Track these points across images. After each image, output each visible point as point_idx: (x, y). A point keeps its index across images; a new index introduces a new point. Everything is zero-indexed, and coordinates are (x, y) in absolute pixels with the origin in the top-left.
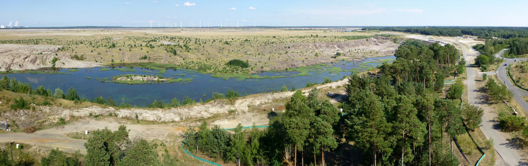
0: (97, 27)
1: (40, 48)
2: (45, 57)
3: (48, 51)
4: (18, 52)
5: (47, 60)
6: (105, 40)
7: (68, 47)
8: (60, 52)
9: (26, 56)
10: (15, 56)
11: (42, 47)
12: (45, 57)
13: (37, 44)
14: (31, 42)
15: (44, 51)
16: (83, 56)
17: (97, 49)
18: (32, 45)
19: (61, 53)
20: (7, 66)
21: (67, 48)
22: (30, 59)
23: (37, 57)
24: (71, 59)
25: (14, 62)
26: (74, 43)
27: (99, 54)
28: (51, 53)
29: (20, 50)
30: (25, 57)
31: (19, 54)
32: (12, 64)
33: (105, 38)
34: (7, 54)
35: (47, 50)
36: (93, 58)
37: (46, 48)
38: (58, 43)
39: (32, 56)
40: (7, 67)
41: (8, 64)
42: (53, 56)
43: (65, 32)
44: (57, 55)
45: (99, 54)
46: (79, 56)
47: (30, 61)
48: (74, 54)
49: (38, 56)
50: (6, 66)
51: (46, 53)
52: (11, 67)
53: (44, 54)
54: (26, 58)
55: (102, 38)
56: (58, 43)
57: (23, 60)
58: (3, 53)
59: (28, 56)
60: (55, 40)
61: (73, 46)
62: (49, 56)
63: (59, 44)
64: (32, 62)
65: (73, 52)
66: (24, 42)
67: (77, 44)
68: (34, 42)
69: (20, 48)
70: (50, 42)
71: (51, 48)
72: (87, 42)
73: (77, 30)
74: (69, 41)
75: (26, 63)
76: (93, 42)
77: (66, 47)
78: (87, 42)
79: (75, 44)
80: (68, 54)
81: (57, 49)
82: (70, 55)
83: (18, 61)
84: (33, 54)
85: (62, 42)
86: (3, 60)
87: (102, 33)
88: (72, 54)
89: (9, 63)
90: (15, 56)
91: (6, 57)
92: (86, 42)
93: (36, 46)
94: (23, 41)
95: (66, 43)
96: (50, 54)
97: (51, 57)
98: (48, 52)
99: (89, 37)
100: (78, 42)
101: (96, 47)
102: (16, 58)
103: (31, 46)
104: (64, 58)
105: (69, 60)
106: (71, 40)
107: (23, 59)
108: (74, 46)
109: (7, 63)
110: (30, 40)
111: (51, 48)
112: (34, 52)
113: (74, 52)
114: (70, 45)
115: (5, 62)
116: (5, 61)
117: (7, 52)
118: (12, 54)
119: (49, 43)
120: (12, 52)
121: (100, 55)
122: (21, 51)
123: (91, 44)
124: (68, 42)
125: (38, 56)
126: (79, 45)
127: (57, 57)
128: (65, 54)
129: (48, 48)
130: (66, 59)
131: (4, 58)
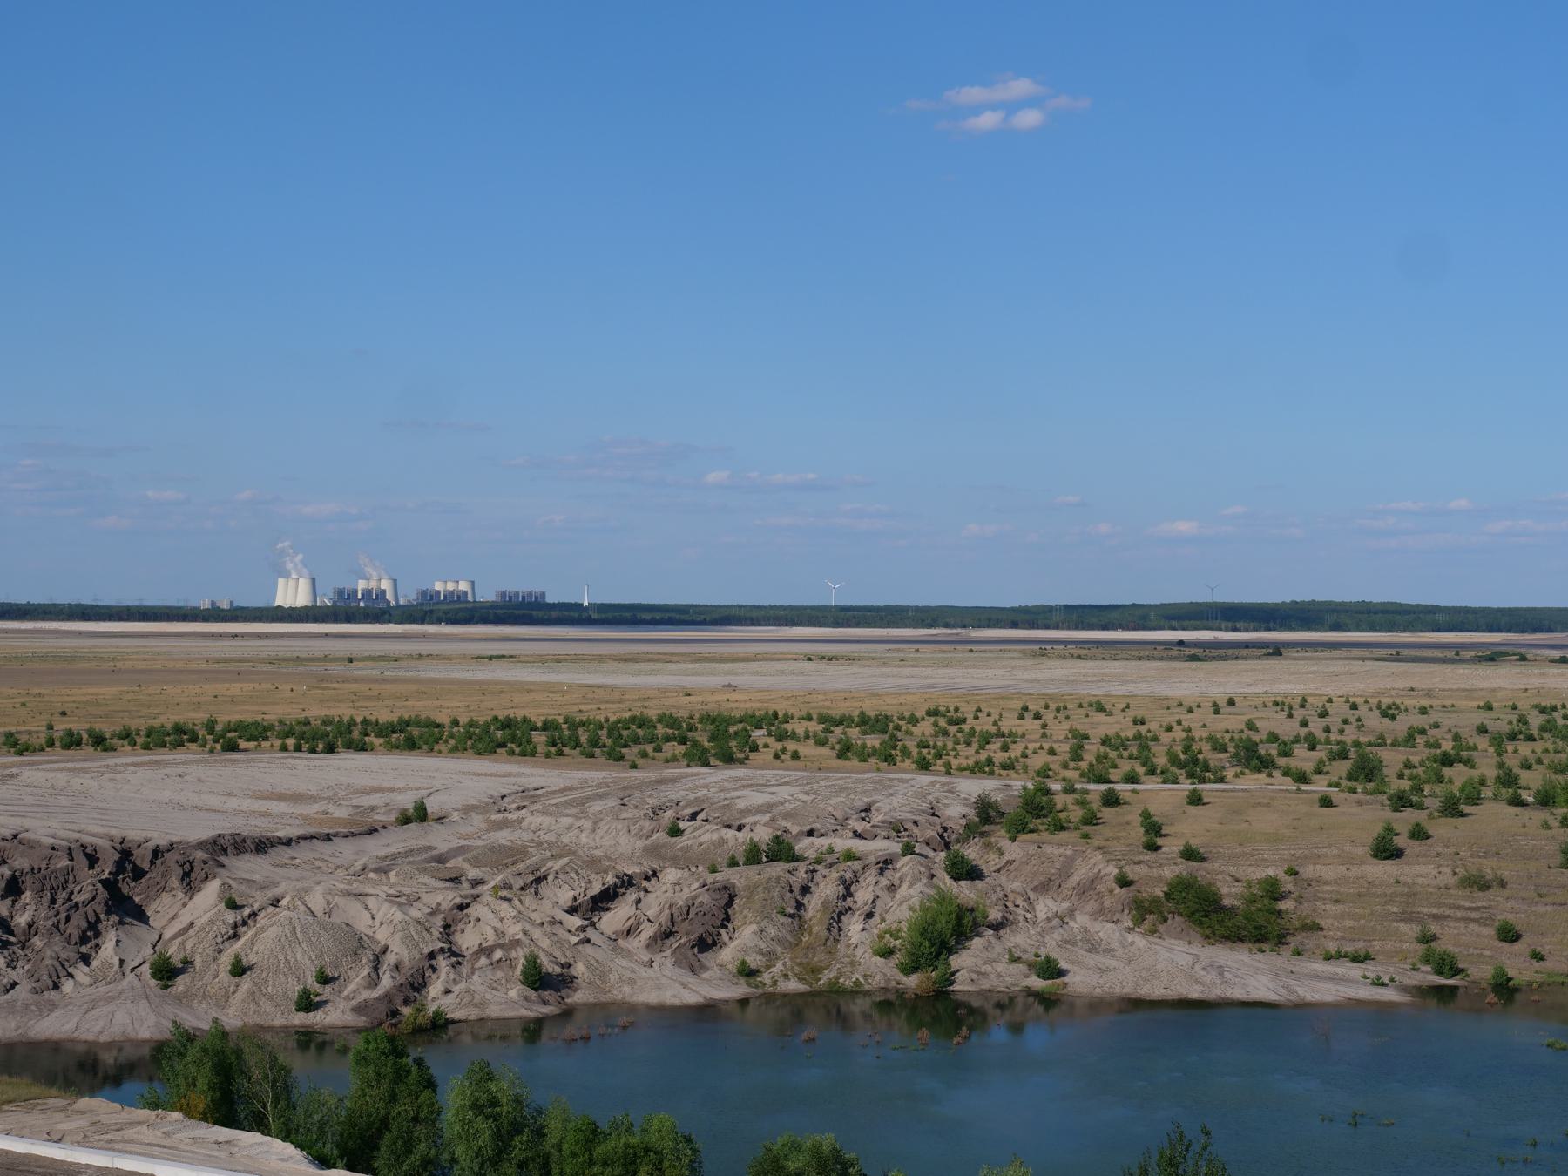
0: (1433, 610)
1: (760, 798)
2: (826, 889)
3: (860, 827)
4: (503, 837)
5: (854, 927)
6: (1539, 746)
7: (1095, 801)
8: (1005, 843)
9: (610, 879)
10: (476, 883)
11: (783, 793)
12: (826, 889)
13: (729, 759)
14: (652, 739)
15: (810, 833)
16: (1273, 891)
17: (1443, 829)
18: (670, 772)
19: (1014, 850)
20: (386, 982)
21: (1082, 803)
22: (657, 902)
23: (729, 897)
24: (1139, 921)
25: (467, 940)
26: (1161, 761)
27: (1479, 883)
28: (895, 847)
29: (533, 820)
30: (596, 889)
31: (517, 853)
32: (443, 963)
33: (1536, 720)
34: (375, 847)
35: (843, 823)
36: (1403, 927)
37: (835, 804)
38: (968, 755)
39: (670, 875)
40: (388, 998)
41: (397, 967)
42: (919, 887)
43: (1042, 650)
44: (965, 871)
45: (1479, 883)
46: (1230, 894)
47: (648, 931)
48: (1167, 869)
49: (739, 877)
50: (373, 982)
51: (843, 843)
52: (434, 990)
53: (811, 854)
54: (605, 899)
55: (1502, 723)
56: (968, 755)
57: (575, 921)
58: (328, 838)
59: (627, 882)
60: (925, 728)
61: (1151, 785)
62: (870, 877)
63: (977, 769)
64: (674, 942)
65: (1153, 847)
66: (578, 745)
67: (1194, 767)
68: (683, 741)
69: (529, 797)
70: (873, 741)
71: (897, 801)
72: (1321, 753)
73: (1181, 643)
74: (1096, 740)
75: (598, 952)
76: (1392, 759)
77: (1070, 798)
78: (1321, 753)
79: (1181, 774)
80: (1095, 865)
81: (956, 812)
82: (1124, 882)
83: (514, 930)
84: (682, 861)
85: (1015, 751)
86: (337, 919)
87: (1503, 680)
88: (1142, 870)
89: (399, 951)
90: (473, 873)
91: (374, 883)
92: (1300, 751)
93: (712, 781)
94: (547, 726)
95: (1064, 749)
96: (885, 864)
97: (892, 888)
98: (857, 835)
99: (1339, 711)
100: (1206, 747)
101: (1434, 804)
102: (486, 898)
103: (653, 775)
104: (1045, 907)
105: (1106, 931)
106: (1103, 726)
107: (572, 910)
108: (1161, 796)
109: (385, 950)
110: (642, 722)
111: (897, 801)
112: (701, 836)
113: (1171, 847)
114: (1115, 775)
115: (357, 943)
116: (362, 923)
117: (372, 831)
118: (441, 859)
119: (864, 756)
120: (439, 839)
121: (1482, 899)
122: (547, 821)
123: (1367, 771)
124: (1091, 750)
125: (739, 877)
126: (1222, 780)
127: (965, 892)
128: (1065, 872)
129: (860, 804)
130: (1081, 920)
131: (348, 894)
